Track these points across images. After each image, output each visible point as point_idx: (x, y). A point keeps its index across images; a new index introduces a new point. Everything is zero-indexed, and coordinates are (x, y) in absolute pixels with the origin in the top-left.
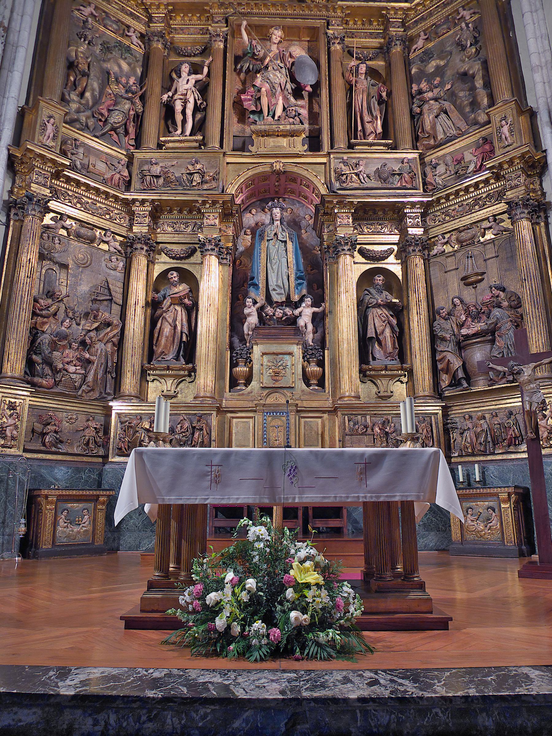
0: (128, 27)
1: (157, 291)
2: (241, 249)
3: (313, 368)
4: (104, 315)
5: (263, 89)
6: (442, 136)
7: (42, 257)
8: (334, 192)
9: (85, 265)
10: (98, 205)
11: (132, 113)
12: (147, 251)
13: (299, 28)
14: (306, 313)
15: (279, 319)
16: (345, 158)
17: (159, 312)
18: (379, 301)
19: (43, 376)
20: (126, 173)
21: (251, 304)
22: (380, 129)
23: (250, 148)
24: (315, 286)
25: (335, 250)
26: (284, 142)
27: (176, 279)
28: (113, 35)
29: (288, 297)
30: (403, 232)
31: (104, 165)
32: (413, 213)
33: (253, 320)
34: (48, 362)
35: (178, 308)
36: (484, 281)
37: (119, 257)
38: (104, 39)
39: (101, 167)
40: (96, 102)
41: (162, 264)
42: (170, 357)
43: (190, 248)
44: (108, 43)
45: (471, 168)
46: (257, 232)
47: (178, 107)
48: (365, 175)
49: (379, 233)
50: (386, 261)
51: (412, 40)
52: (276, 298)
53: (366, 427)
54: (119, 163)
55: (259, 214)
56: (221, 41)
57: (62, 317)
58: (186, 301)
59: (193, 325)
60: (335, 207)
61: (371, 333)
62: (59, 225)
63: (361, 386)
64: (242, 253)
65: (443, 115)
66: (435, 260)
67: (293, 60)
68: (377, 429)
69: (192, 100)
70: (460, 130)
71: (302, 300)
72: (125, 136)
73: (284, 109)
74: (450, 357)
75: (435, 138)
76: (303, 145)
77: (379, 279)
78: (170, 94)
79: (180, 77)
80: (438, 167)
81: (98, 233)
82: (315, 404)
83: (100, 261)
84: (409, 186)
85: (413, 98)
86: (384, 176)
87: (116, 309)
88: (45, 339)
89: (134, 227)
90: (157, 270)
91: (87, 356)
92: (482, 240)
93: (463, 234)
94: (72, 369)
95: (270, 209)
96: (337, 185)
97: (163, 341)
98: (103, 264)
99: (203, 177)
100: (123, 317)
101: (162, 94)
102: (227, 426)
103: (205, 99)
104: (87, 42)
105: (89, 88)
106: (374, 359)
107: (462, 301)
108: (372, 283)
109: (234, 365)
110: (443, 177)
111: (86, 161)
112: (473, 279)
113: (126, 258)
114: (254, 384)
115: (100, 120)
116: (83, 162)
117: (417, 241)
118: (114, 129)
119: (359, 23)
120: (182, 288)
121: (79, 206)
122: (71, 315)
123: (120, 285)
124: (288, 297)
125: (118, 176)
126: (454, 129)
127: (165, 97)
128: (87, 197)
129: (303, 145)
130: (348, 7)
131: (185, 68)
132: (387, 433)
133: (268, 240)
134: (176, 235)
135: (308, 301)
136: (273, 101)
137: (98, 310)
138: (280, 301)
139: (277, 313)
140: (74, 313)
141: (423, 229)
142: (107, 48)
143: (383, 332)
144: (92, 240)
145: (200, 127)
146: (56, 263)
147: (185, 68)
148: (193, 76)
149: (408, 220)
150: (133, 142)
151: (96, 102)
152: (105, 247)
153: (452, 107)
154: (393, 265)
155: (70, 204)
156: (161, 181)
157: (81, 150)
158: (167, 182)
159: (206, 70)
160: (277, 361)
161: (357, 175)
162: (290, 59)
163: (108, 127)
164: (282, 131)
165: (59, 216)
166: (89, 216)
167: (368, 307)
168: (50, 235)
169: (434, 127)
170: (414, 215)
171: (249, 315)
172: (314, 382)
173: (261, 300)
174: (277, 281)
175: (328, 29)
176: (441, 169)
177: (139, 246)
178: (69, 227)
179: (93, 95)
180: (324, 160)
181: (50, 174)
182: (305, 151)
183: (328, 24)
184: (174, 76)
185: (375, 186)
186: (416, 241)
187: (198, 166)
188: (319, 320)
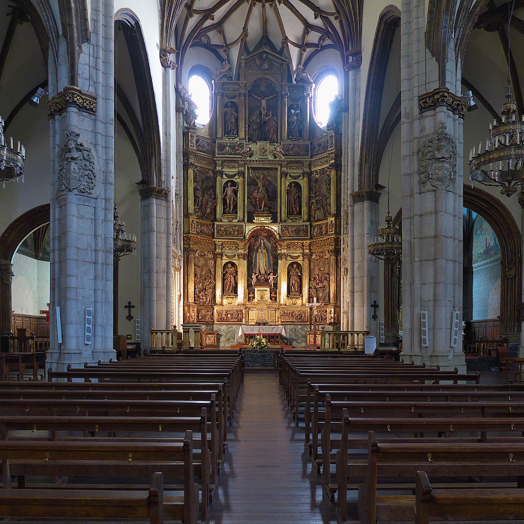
11: (213, 207)
22: (298, 210)
25: (281, 256)
33: (254, 280)
40: (202, 205)
75: (314, 219)
90: (224, 262)
108: (293, 267)
109: (249, 294)
114: (256, 300)
124: (266, 272)
131: (229, 184)
147: (229, 184)
154: (300, 260)
172: (273, 299)
187: (237, 228)
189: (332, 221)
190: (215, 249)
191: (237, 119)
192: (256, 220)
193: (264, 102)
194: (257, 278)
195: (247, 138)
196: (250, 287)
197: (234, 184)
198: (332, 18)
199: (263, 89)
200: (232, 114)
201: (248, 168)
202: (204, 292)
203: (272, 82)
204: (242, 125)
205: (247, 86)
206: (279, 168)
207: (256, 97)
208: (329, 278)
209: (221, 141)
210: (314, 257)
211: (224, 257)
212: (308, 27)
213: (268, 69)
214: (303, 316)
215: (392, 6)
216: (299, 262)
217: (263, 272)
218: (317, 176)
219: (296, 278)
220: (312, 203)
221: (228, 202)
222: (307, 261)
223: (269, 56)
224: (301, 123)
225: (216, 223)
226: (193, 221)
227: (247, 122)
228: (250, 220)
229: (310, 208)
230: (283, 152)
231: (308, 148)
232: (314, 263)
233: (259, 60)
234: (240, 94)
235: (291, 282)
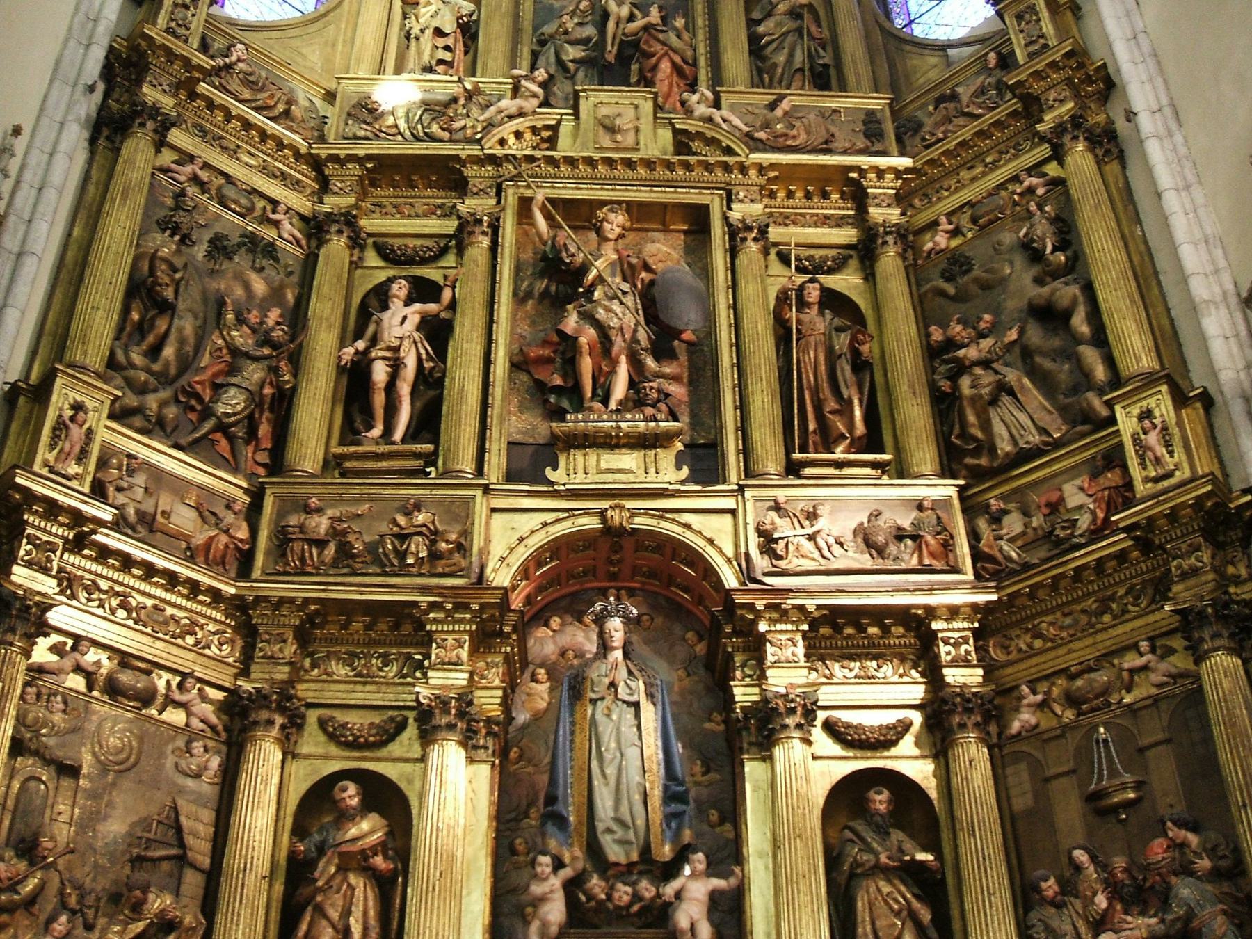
0: (274, 203)
1: (299, 831)
2: (521, 717)
4: (158, 902)
5: (583, 340)
6: (1008, 448)
8: (755, 581)
9: (120, 768)
10: (170, 611)
11: (268, 391)
12: (283, 727)
13: (664, 206)
14: (694, 891)
16: (781, 499)
17: (305, 891)
18: (883, 859)
20: (243, 533)
21: (548, 870)
22: (860, 428)
23: (549, 472)
24: (714, 816)
25: (766, 726)
26: (629, 460)
27: (354, 802)
28: (238, 220)
29: (646, 850)
30: (933, 675)
31: (193, 514)
32: (953, 630)
36: (1145, 805)
37: (211, 744)
38: (218, 228)
39: (184, 518)
40: (186, 364)
41: (319, 759)
43: (392, 719)
44: (226, 237)
45: (1084, 522)
47: (380, 372)
48: (831, 541)
49: (869, 679)
50: (894, 751)
52: (615, 853)
54: (228, 507)
55: (569, 629)
56: (484, 233)
57: (49, 908)
58: (379, 861)
59: (395, 924)
60: (758, 615)
62: (68, 663)
64: (525, 727)
65: (1006, 399)
66: (1016, 747)
67: (651, 276)
69: (411, 363)
70: (1049, 435)
71: (682, 856)
72: (248, 443)
75: (992, 449)
76: (679, 468)
78: (361, 345)
80: (1006, 520)
81: (161, 681)
83: (162, 755)
84: (938, 565)
87: (193, 882)
89: (253, 668)
93: (1079, 683)
95: (600, 620)
96: (761, 563)
98: (169, 762)
99: (433, 542)
101: (342, 344)
104: (177, 238)
105: (173, 337)
107: (1093, 858)
110: (1020, 543)
111: (148, 506)
113: (228, 743)
115: (192, 409)
116: (143, 507)
117: (969, 701)
118: (222, 428)
119: (799, 194)
120: (367, 829)
121: (122, 614)
122: (73, 901)
123: (208, 815)
124: (646, 850)
125: (224, 539)
126: (1034, 431)
128: (143, 593)
129: (679, 468)
130: (773, 166)
133: (594, 702)
134: (359, 687)
137: (145, 890)
138: (623, 860)
139: (616, 895)
140: (81, 897)
141: (980, 671)
142: (220, 248)
144: (147, 698)
145: (428, 422)
146: (48, 762)
147: (400, 289)
148: (417, 306)
149: (943, 649)
150: (263, 457)
151: (186, 364)
152: (176, 717)
153: (1026, 381)
155: (100, 611)
157: (140, 479)
158: (345, 551)
159: (447, 294)
161: (811, 538)
162: (643, 275)
163: (208, 425)
164: (627, 435)
165: (70, 642)
166: (146, 639)
167: (852, 876)
168: (44, 691)
169: (986, 425)
170: (957, 635)
171: (542, 899)
173: (575, 855)
174: (617, 807)
175: (730, 208)
176: (1013, 524)
177: (264, 715)
178: (91, 669)
179: (179, 353)
180: (729, 503)
181: (60, 542)
182: (683, 482)
183: (730, 201)
184: (374, 302)
185: (856, 566)
186: (966, 700)
187: (421, 518)
201: (525, 204)
210: (1023, 719)
211: (312, 741)
218: (955, 243)
220: (961, 368)
222: (973, 756)
228: (530, 465)
232: (1036, 767)
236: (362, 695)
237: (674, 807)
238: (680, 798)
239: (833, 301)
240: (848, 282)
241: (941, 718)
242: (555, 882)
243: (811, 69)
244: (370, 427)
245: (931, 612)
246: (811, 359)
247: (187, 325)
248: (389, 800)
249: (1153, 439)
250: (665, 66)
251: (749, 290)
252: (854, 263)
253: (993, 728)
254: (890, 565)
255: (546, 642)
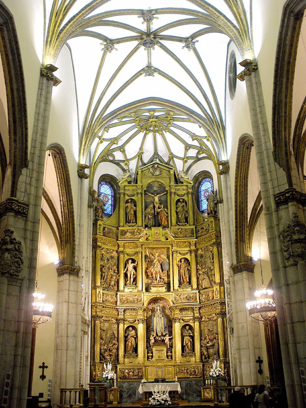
0: (113, 250)
1: (126, 332)
3: (169, 354)
5: (154, 273)
7: (100, 329)
11: (116, 280)
14: (167, 338)
15: (160, 341)
17: (127, 339)
19: (102, 360)
20: (116, 299)
22: (188, 280)
29: (162, 334)
30: (194, 313)
33: (153, 341)
34: (104, 357)
35: (133, 338)
42: (131, 352)
45: (211, 298)
46: (153, 310)
49: (187, 314)
51: (197, 249)
53: (182, 371)
58: (135, 336)
61: (185, 344)
63: (182, 358)
64: (148, 318)
68: (185, 371)
69: (132, 273)
73: (160, 278)
74: (204, 351)
75: (202, 287)
77: (187, 327)
79: (128, 263)
82: (170, 364)
85: (198, 270)
86: (188, 298)
87: (116, 339)
88: (103, 351)
91: (111, 354)
92: (213, 319)
94: (108, 357)
95: (157, 306)
97: (129, 348)
100: (118, 341)
102: (147, 370)
103: (136, 272)
106: (186, 351)
108: (186, 328)
109: (148, 353)
112: (211, 330)
123: (117, 332)
124: (162, 334)
127: (125, 271)
132: (188, 372)
135: (167, 335)
136: (157, 275)
143: (188, 343)
145: (135, 280)
147: (130, 261)
150: (116, 288)
151: (107, 278)
156: (126, 302)
159: (136, 263)
160: (159, 352)
172: (170, 357)
173: (155, 335)
177: (121, 321)
183: (172, 247)
187: (136, 297)
188: (171, 340)
189: (217, 289)
190: (118, 315)
191: (135, 212)
192: (153, 289)
193: (157, 199)
194: (155, 339)
195: (144, 225)
196: (148, 347)
197: (133, 261)
198: (205, 140)
199: (155, 189)
200: (132, 208)
202: (109, 352)
203: (162, 184)
204: (139, 215)
205: (143, 187)
206: (171, 248)
207: (150, 194)
208: (218, 337)
209: (123, 228)
210: (203, 319)
212: (188, 147)
213: (159, 175)
214: (197, 372)
215: (246, 134)
216: (190, 324)
217: (159, 334)
218: (202, 253)
219: (188, 338)
220: (200, 274)
221: (129, 276)
223: (160, 166)
224: (187, 212)
225: (119, 293)
226: (99, 292)
227: (144, 213)
229: (198, 278)
230: (173, 235)
231: (193, 231)
232: (204, 325)
233: (152, 169)
234: (137, 194)
235: (184, 342)
236: (131, 317)
237: (165, 329)
238: (166, 328)
239: (186, 260)
240: (188, 256)
241: (194, 318)
242: (153, 338)
243: (185, 217)
244: (128, 281)
245: (193, 308)
246: (182, 271)
247: (106, 274)
248: (134, 328)
249: (217, 292)
250: (164, 218)
251: (175, 261)
252: (189, 253)
253: (200, 320)
254: (189, 302)
255: (151, 307)
